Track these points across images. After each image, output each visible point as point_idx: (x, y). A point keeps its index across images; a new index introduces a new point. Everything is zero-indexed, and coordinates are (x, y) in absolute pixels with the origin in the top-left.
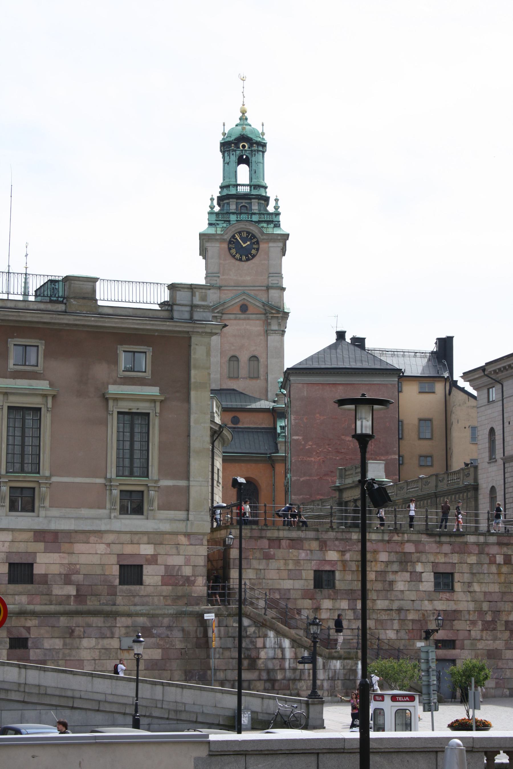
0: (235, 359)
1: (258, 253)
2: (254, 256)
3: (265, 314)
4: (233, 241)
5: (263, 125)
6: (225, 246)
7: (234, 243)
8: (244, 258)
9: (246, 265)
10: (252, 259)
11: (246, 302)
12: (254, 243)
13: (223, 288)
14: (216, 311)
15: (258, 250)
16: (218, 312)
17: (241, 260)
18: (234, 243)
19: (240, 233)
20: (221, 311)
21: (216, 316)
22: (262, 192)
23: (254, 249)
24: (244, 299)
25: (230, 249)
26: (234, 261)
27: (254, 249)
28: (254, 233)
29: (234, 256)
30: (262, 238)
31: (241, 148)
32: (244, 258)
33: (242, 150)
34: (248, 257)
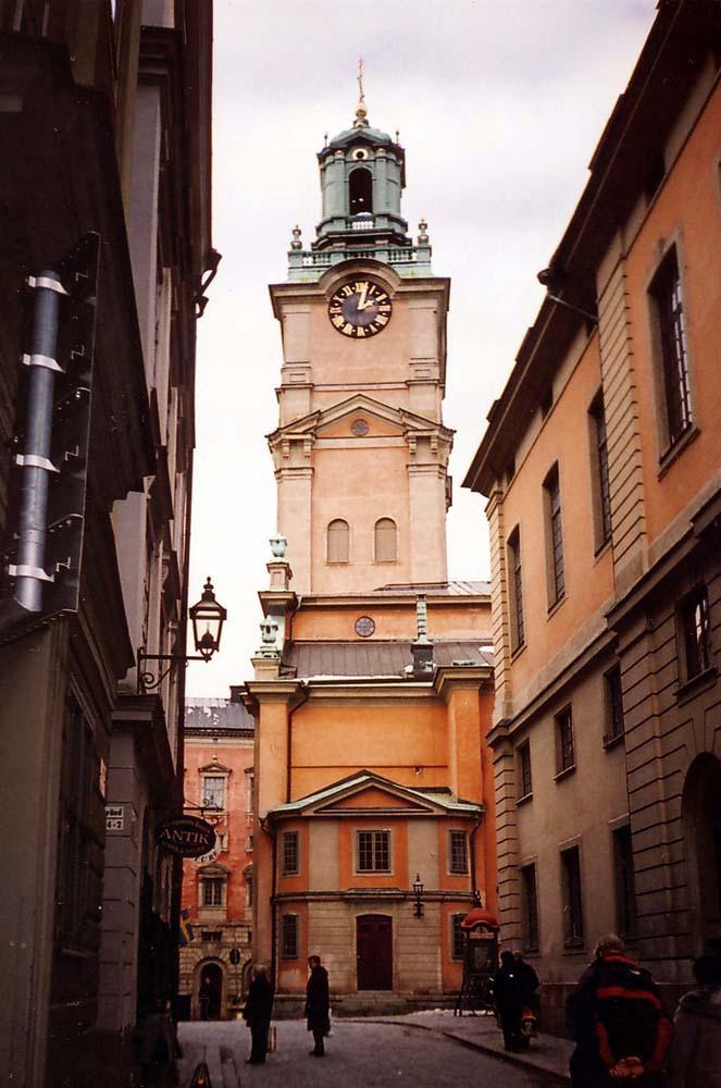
0: (339, 525)
1: (390, 323)
2: (381, 328)
4: (338, 302)
5: (397, 133)
8: (361, 332)
10: (376, 333)
11: (363, 415)
12: (380, 303)
13: (317, 388)
14: (297, 431)
15: (389, 314)
16: (304, 433)
17: (354, 336)
18: (340, 305)
19: (352, 285)
20: (312, 431)
21: (302, 441)
22: (398, 229)
23: (380, 313)
24: (360, 408)
25: (332, 316)
27: (380, 313)
28: (382, 285)
29: (340, 330)
31: (355, 158)
32: (361, 332)
33: (357, 161)
34: (369, 329)
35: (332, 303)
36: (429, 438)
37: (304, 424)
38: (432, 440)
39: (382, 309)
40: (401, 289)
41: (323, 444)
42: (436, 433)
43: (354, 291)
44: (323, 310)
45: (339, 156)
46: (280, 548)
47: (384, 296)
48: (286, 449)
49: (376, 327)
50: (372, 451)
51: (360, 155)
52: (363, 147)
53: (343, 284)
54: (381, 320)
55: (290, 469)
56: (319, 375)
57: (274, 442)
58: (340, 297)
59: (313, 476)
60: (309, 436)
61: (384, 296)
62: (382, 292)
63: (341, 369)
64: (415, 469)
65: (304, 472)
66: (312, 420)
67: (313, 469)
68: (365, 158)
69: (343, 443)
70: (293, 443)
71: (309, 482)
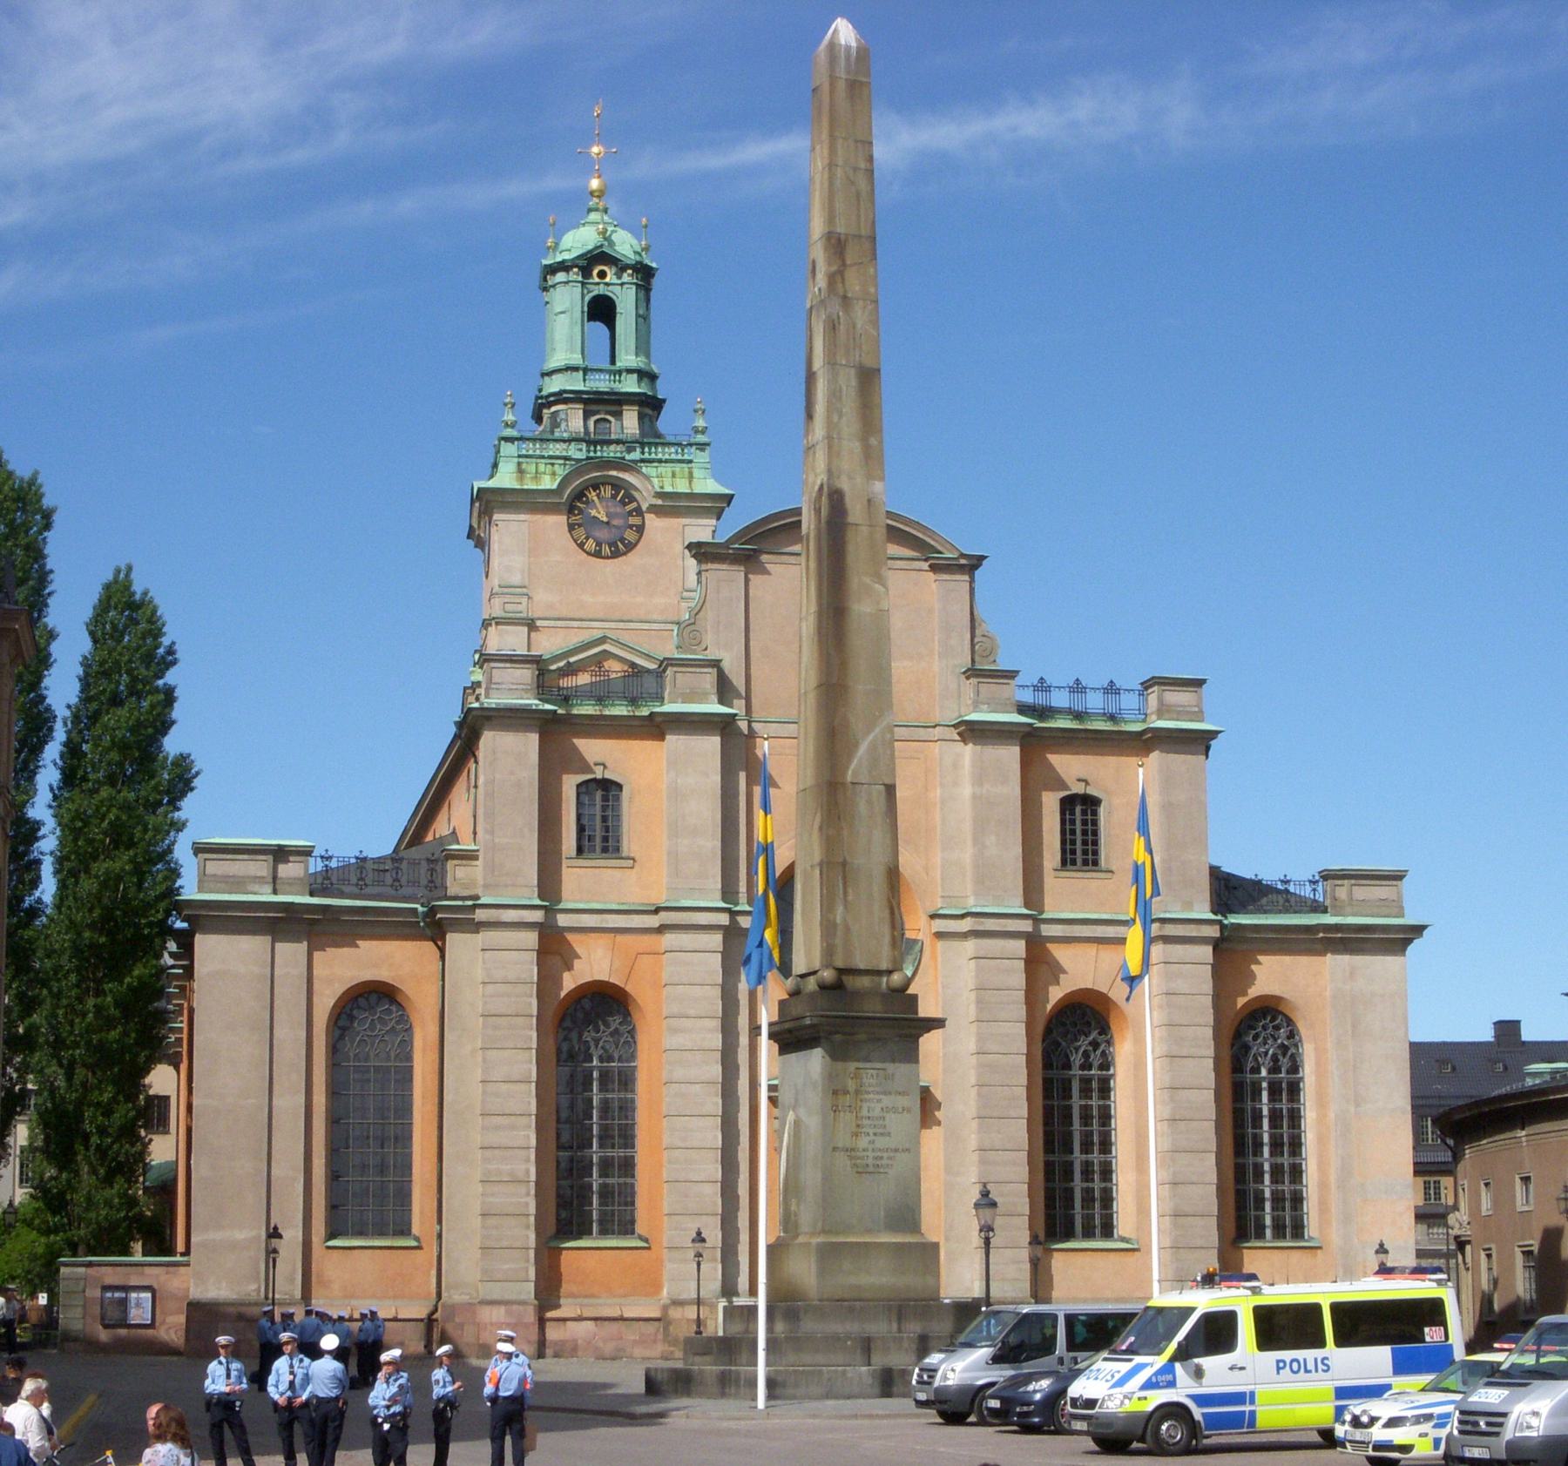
2: (630, 547)
9: (609, 568)
10: (625, 554)
12: (630, 513)
15: (640, 529)
17: (597, 554)
27: (631, 527)
29: (581, 546)
32: (606, 550)
33: (598, 284)
39: (632, 521)
44: (563, 519)
45: (574, 277)
47: (634, 505)
49: (623, 543)
51: (602, 275)
52: (606, 265)
54: (630, 536)
58: (583, 503)
61: (634, 505)
68: (607, 280)
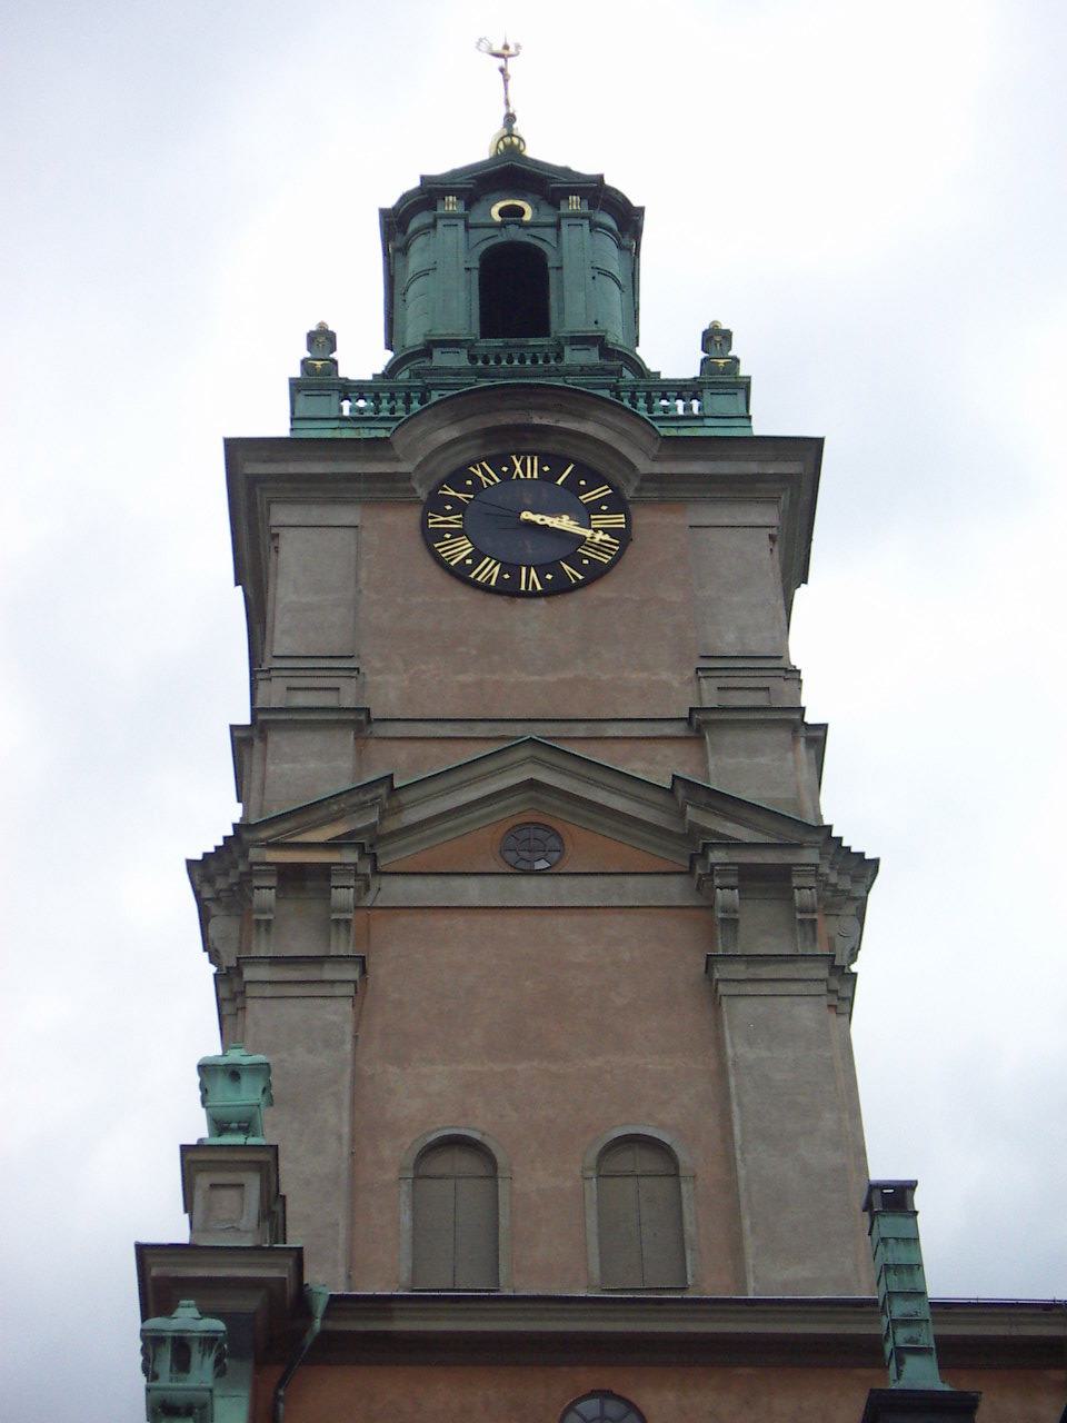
2: (595, 573)
3: (691, 872)
6: (405, 521)
7: (459, 506)
8: (530, 578)
10: (580, 585)
12: (594, 508)
13: (381, 730)
17: (508, 590)
18: (459, 506)
21: (325, 871)
24: (532, 784)
25: (431, 537)
26: (463, 595)
29: (460, 574)
30: (645, 466)
35: (435, 504)
36: (785, 872)
37: (333, 819)
38: (796, 881)
40: (658, 468)
41: (396, 890)
42: (810, 856)
43: (506, 477)
44: (405, 521)
46: (248, 1094)
48: (266, 897)
50: (577, 918)
53: (472, 454)
55: (276, 961)
56: (387, 692)
57: (221, 884)
59: (360, 992)
60: (351, 856)
62: (596, 479)
63: (468, 678)
64: (740, 971)
65: (329, 973)
66: (362, 806)
67: (362, 962)
69: (472, 891)
70: (292, 878)
71: (347, 1006)
